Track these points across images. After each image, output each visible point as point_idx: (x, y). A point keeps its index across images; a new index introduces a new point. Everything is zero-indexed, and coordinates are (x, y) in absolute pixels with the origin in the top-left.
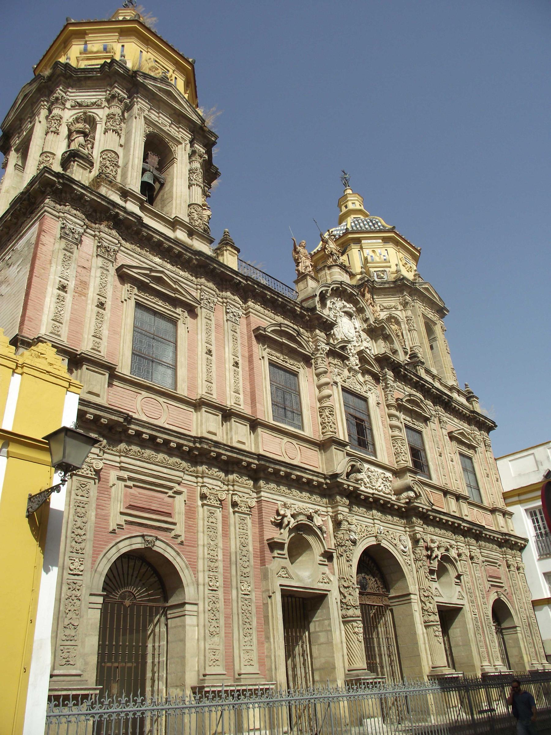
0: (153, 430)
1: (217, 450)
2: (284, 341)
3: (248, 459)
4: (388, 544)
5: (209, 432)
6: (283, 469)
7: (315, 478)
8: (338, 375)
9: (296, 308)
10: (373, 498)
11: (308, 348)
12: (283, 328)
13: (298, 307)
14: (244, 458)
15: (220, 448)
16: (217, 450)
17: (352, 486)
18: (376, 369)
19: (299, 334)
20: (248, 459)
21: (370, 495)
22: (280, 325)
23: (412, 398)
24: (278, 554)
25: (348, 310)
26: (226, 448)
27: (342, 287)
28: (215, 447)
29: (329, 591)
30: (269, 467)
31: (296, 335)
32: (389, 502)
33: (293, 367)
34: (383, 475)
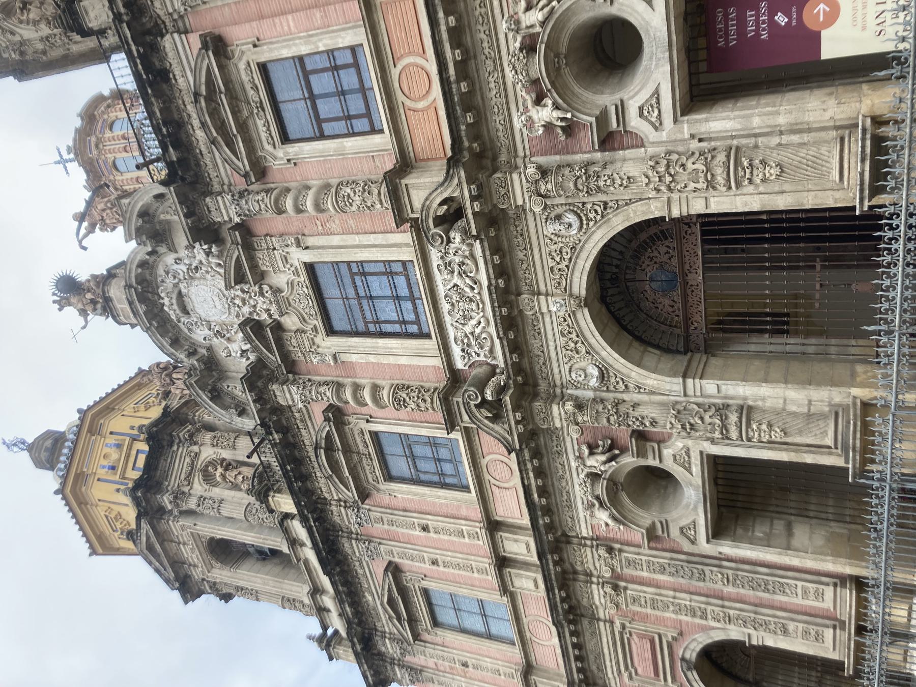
0: (569, 660)
1: (559, 605)
2: (348, 474)
3: (552, 567)
4: (577, 274)
5: (537, 586)
6: (541, 522)
7: (529, 466)
8: (314, 344)
9: (278, 441)
10: (505, 334)
11: (324, 427)
12: (331, 473)
13: (274, 439)
14: (553, 572)
15: (555, 603)
16: (559, 605)
17: (515, 417)
18: (237, 252)
19: (317, 447)
20: (552, 567)
21: (505, 343)
22: (329, 478)
23: (215, 134)
24: (663, 532)
25: (178, 312)
26: (551, 596)
27: (151, 324)
28: (556, 607)
29: (701, 453)
30: (549, 541)
31: (322, 451)
32: (496, 288)
33: (367, 441)
34: (447, 277)
